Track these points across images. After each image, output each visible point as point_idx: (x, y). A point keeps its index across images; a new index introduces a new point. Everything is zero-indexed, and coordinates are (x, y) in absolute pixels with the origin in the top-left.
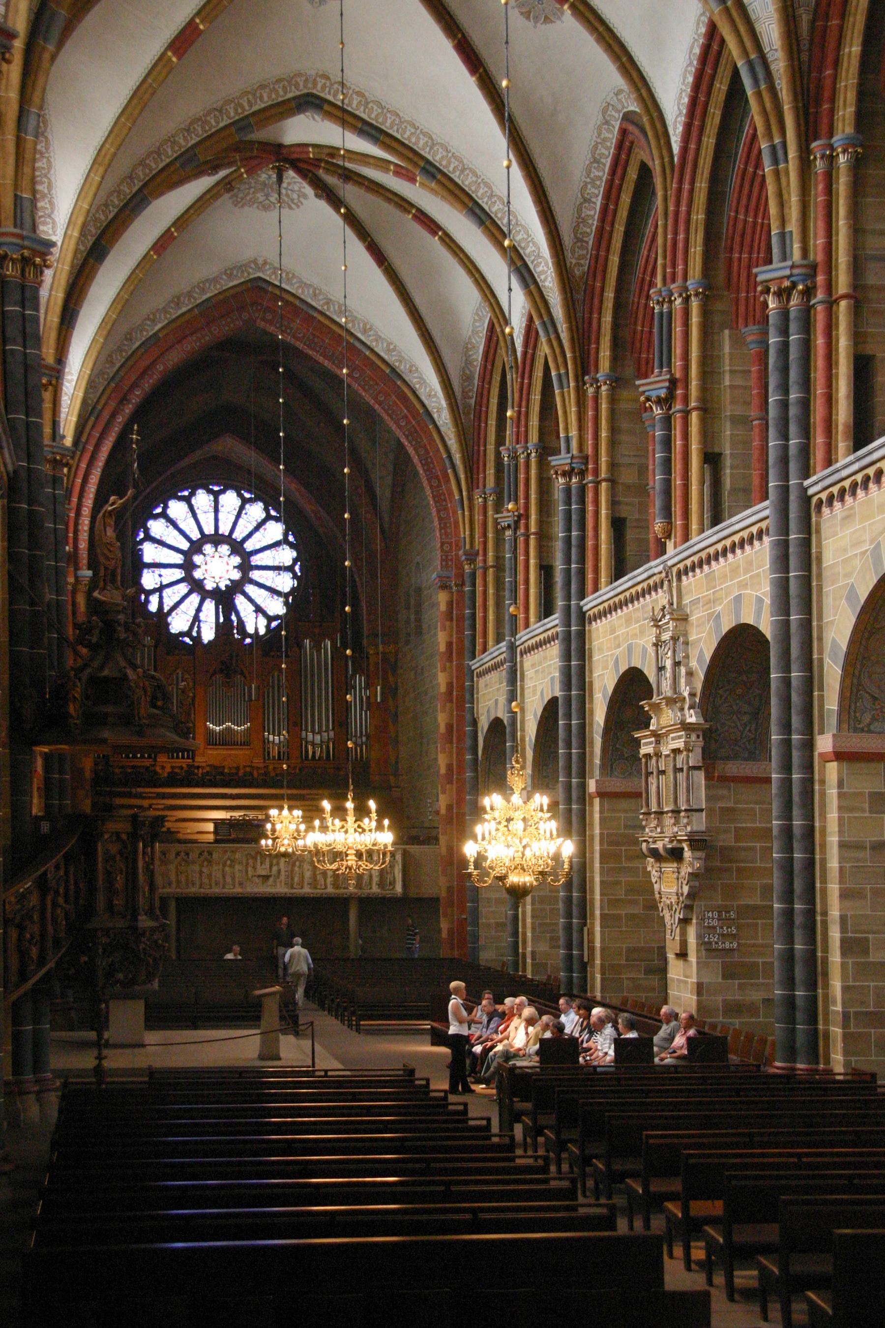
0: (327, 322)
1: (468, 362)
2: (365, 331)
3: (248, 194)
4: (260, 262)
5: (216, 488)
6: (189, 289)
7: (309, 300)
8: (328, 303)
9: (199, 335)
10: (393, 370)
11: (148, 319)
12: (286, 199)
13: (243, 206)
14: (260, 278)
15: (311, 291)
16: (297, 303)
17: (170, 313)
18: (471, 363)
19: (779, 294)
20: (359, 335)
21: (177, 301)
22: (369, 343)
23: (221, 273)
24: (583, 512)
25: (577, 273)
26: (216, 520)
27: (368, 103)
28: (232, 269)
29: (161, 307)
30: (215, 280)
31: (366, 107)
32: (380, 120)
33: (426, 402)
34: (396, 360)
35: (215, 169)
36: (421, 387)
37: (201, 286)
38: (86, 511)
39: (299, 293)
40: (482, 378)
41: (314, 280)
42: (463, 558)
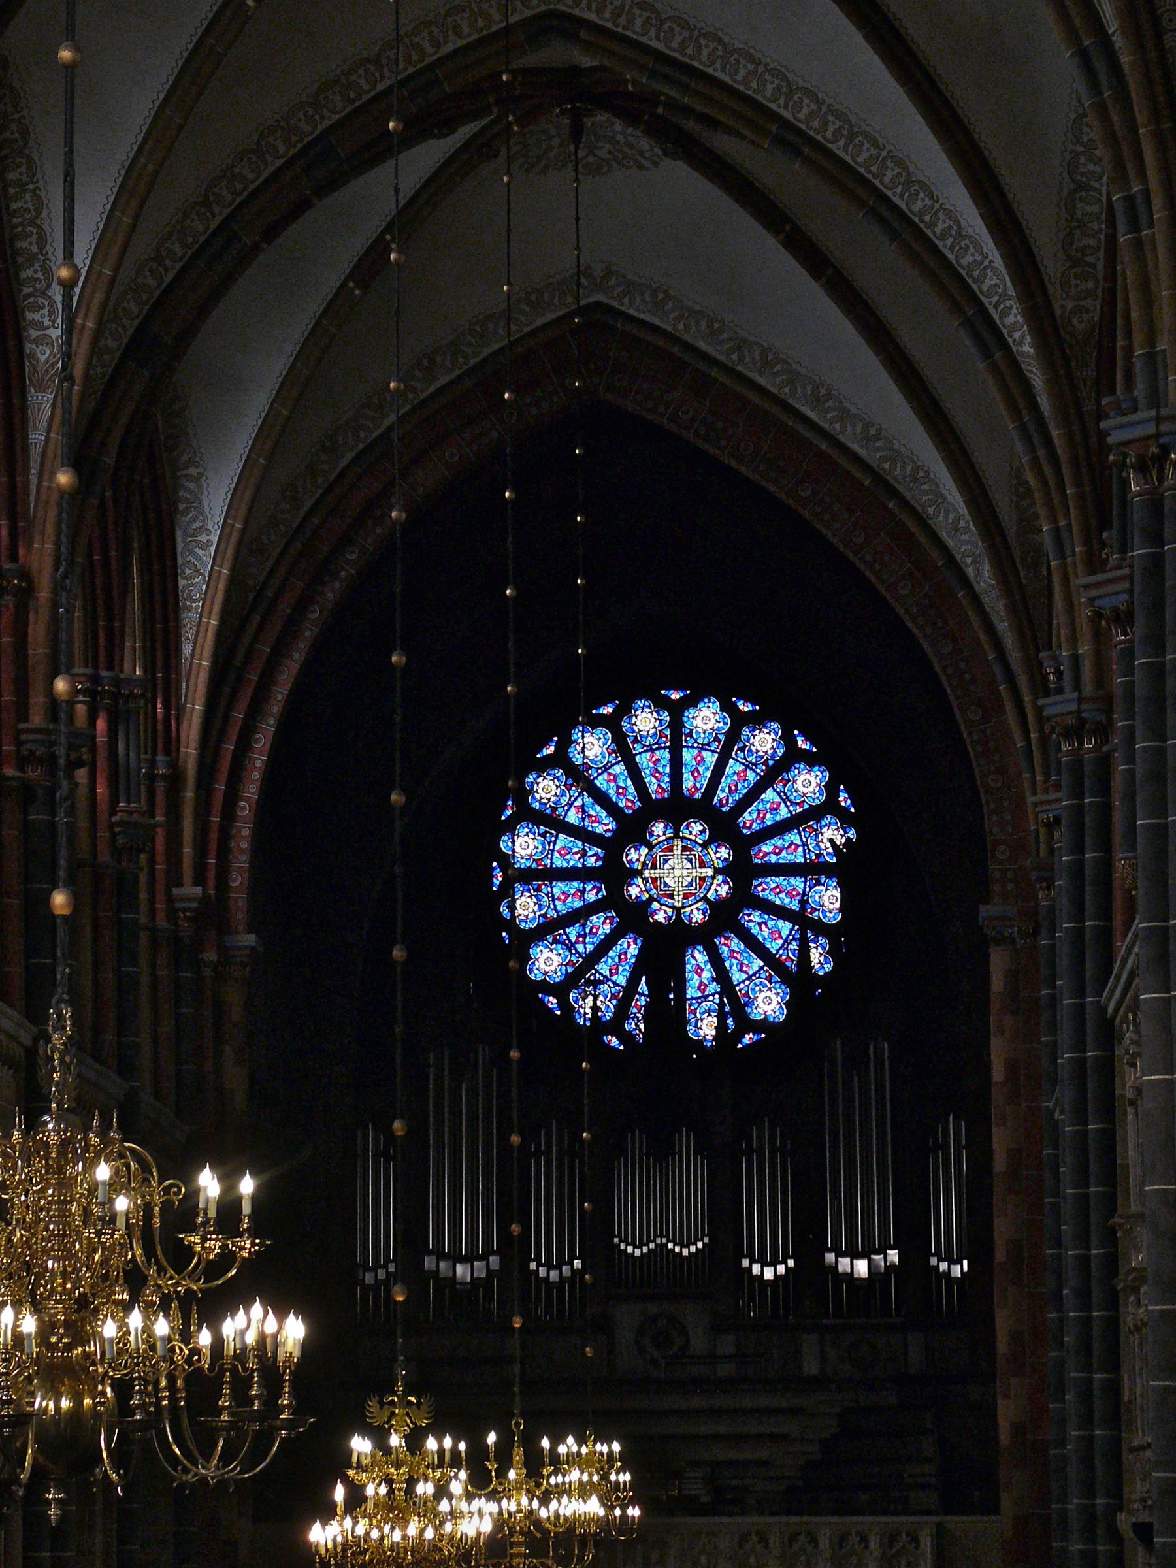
2: (817, 401)
5: (675, 696)
8: (739, 348)
10: (878, 478)
14: (598, 304)
19: (1142, 468)
20: (807, 411)
24: (1105, 809)
25: (1079, 325)
26: (676, 763)
27: (662, 22)
31: (659, 29)
32: (689, 51)
34: (884, 459)
35: (447, 126)
36: (937, 512)
38: (245, 809)
42: (1034, 876)
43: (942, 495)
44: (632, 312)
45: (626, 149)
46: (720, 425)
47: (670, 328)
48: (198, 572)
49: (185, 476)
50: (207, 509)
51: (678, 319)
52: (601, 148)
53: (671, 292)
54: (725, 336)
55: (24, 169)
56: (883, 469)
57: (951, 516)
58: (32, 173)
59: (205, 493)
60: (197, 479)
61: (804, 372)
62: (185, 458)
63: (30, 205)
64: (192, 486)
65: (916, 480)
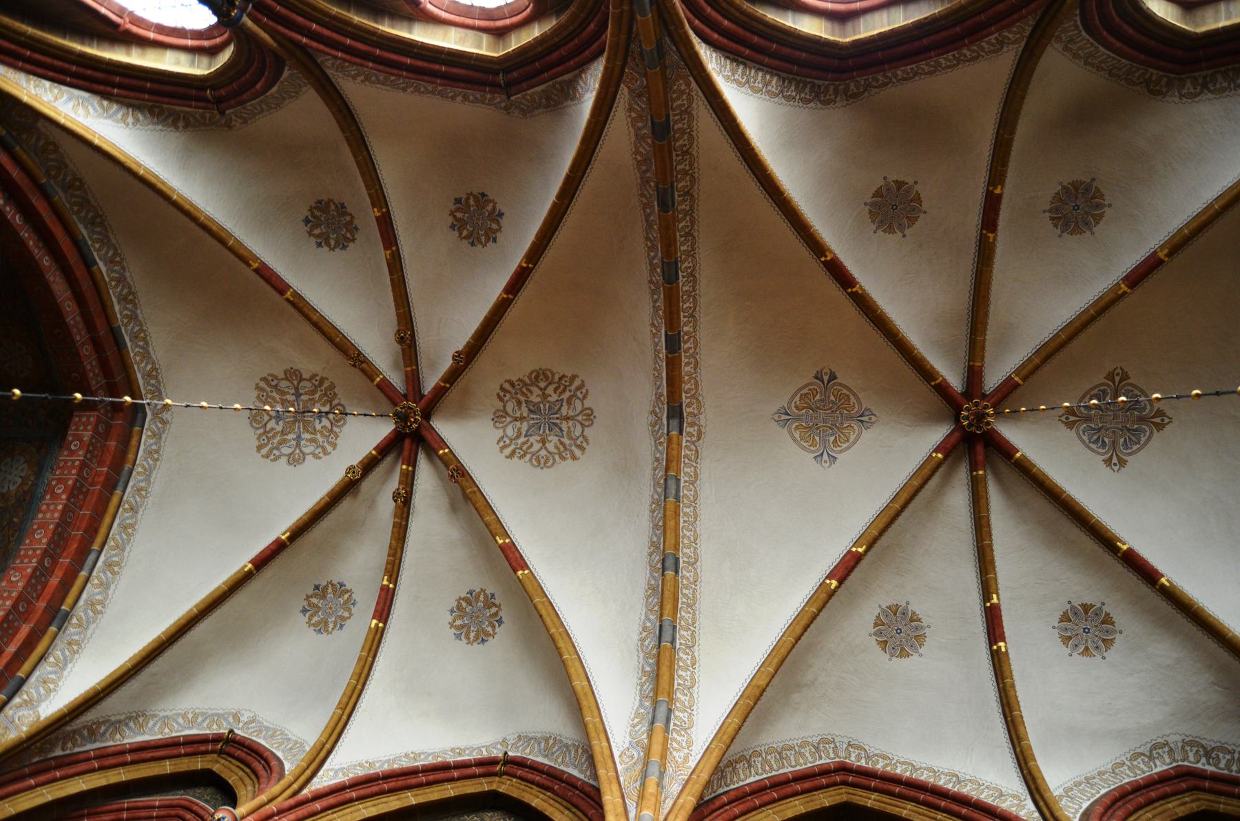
0: (111, 509)
1: (117, 726)
2: (109, 565)
3: (283, 393)
4: (165, 416)
6: (140, 317)
7: (131, 483)
9: (81, 326)
10: (67, 616)
11: (116, 254)
12: (275, 441)
13: (258, 387)
15: (143, 484)
16: (128, 466)
17: (116, 286)
18: (117, 730)
20: (102, 558)
21: (129, 298)
22: (94, 574)
23: (153, 363)
27: (693, 484)
28: (156, 378)
29: (127, 274)
30: (146, 355)
33: (33, 679)
34: (79, 619)
37: (141, 336)
39: (138, 469)
40: (102, 755)
41: (156, 487)
43: (66, 665)
44: (144, 437)
45: (278, 438)
46: (81, 497)
47: (138, 462)
48: (56, 99)
49: (128, 113)
50: (102, 120)
51: (143, 467)
52: (277, 424)
53: (158, 463)
54: (138, 499)
55: (774, 89)
56: (71, 619)
57: (53, 676)
58: (768, 92)
59: (114, 124)
60: (124, 120)
61: (126, 554)
62: (140, 116)
63: (756, 85)
64: (119, 116)
65: (69, 644)
